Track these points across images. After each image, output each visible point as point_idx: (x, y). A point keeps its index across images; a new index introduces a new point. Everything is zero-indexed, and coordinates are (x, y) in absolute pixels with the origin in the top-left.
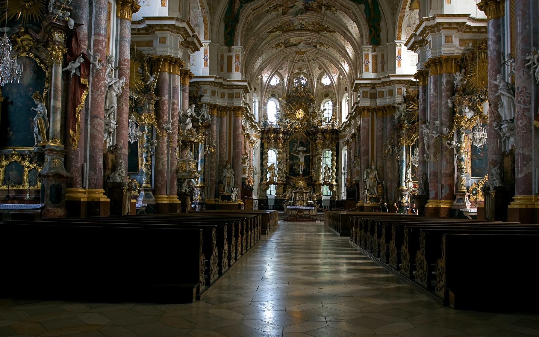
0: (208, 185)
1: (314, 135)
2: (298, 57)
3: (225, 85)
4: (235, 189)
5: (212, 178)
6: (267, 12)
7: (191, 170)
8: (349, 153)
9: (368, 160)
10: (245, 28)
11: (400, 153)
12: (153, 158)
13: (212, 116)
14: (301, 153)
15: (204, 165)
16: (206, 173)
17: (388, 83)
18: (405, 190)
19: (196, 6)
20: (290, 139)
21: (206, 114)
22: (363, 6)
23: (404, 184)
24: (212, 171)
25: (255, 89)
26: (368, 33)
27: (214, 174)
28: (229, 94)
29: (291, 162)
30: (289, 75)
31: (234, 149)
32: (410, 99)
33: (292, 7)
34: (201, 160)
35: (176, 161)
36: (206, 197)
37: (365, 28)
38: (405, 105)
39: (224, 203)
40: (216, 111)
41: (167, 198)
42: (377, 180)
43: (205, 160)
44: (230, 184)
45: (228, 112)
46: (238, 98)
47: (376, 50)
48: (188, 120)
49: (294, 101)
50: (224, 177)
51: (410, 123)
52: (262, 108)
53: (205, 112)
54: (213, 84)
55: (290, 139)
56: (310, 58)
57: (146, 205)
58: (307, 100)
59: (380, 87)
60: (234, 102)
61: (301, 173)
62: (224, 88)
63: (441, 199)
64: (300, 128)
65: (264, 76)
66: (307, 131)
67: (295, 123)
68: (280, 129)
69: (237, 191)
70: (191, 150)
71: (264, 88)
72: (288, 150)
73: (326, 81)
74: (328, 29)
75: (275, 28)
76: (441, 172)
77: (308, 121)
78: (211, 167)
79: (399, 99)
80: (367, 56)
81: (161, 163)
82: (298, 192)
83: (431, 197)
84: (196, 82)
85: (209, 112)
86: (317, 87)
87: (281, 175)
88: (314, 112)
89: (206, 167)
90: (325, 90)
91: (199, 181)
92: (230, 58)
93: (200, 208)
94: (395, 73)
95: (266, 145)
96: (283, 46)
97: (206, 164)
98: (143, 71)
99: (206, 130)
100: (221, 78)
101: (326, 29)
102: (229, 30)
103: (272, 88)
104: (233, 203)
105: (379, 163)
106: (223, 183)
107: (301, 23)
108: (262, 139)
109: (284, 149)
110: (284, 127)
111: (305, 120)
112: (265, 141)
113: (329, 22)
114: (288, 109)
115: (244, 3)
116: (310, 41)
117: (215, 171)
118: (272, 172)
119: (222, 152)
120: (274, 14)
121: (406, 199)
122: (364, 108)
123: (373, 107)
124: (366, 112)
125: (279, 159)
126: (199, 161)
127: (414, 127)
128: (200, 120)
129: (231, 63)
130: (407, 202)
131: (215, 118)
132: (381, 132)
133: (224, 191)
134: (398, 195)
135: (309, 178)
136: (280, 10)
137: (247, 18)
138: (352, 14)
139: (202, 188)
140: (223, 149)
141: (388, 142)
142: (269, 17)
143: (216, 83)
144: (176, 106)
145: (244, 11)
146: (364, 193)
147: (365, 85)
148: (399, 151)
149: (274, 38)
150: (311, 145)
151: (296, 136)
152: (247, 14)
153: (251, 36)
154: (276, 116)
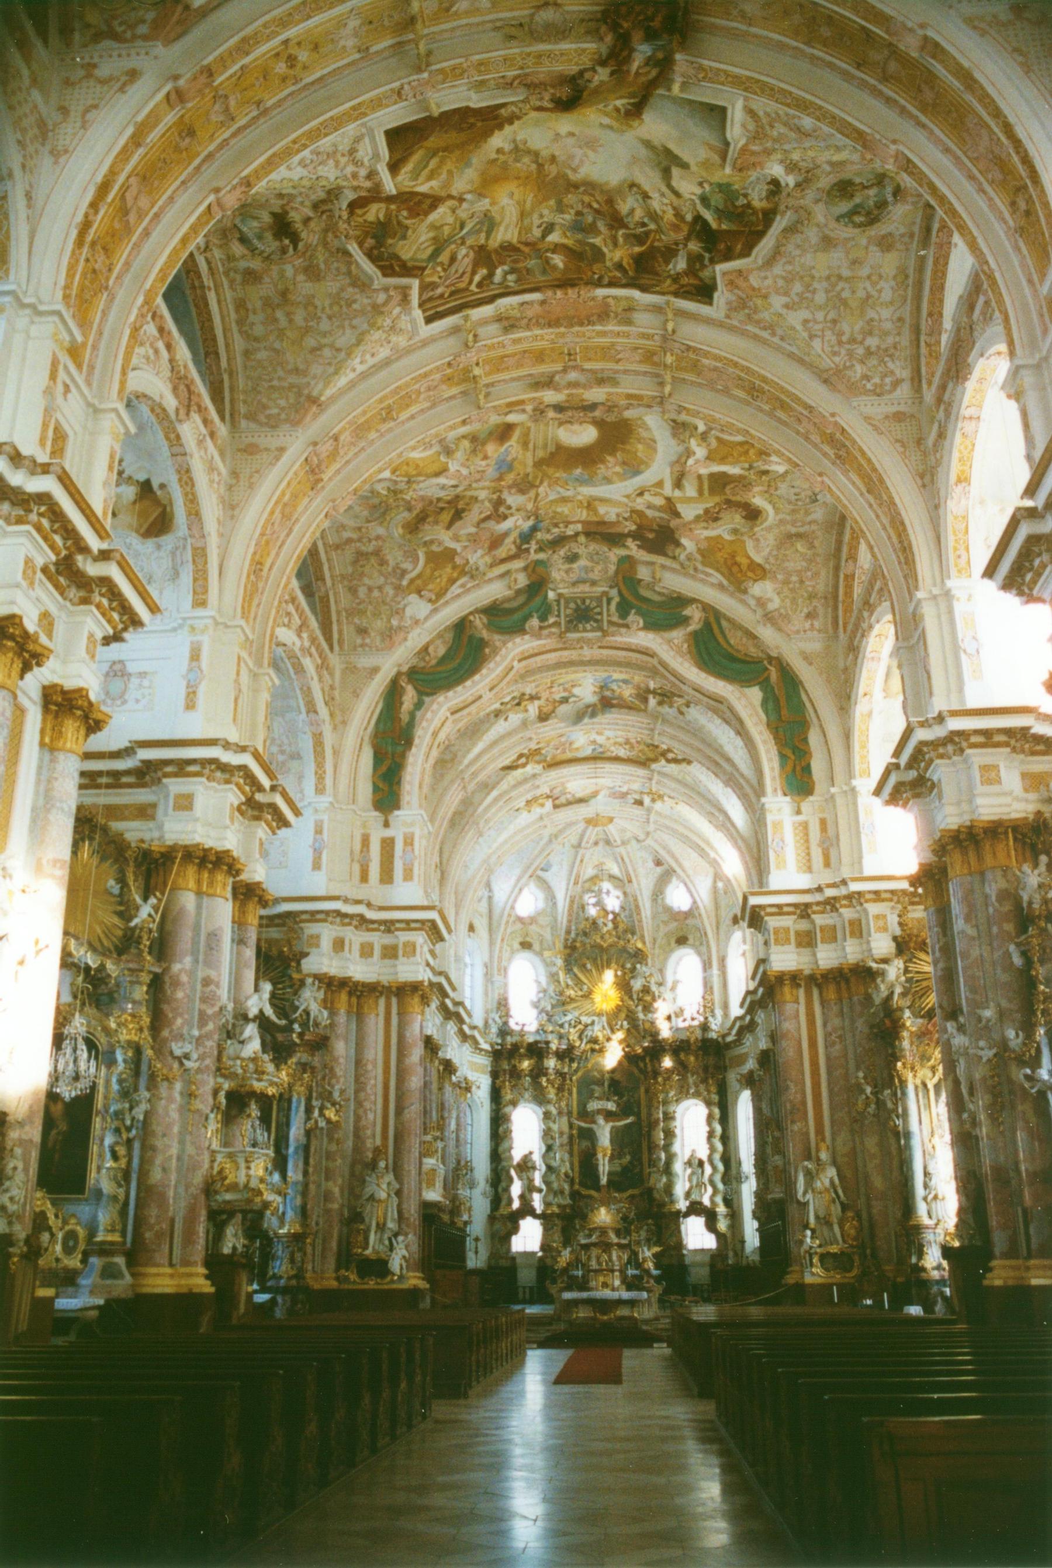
0: (315, 1229)
1: (651, 1061)
2: (592, 833)
3: (373, 922)
4: (401, 1238)
5: (330, 1206)
6: (497, 716)
7: (253, 1184)
8: (758, 1110)
9: (807, 1134)
10: (431, 761)
11: (900, 1110)
12: (137, 1145)
13: (333, 1013)
14: (601, 1120)
15: (306, 1163)
16: (312, 1187)
17: (844, 902)
18: (927, 1228)
19: (293, 703)
20: (580, 1074)
21: (314, 1008)
22: (755, 694)
23: (922, 1208)
24: (330, 1184)
25: (471, 928)
26: (776, 764)
27: (336, 1190)
28: (385, 948)
29: (585, 1144)
31: (399, 1111)
32: (912, 945)
33: (565, 700)
34: (297, 1149)
35: (206, 1158)
36: (310, 1268)
37: (768, 751)
38: (899, 964)
39: (366, 1287)
40: (344, 996)
41: (172, 1276)
42: (838, 1197)
43: (306, 1148)
44: (384, 1224)
45: (382, 1002)
46: (412, 959)
47: (803, 809)
48: (251, 1030)
50: (368, 1200)
51: (922, 1017)
52: (492, 983)
53: (310, 1000)
54: (338, 920)
55: (580, 1074)
56: (628, 835)
57: (101, 1302)
59: (822, 912)
60: (400, 968)
61: (604, 1180)
62: (368, 930)
63: (1029, 1256)
65: (495, 887)
67: (593, 1023)
68: (547, 1043)
69: (407, 1247)
70: (265, 1120)
71: (500, 924)
73: (678, 898)
74: (670, 756)
75: (521, 756)
76: (1018, 1170)
77: (631, 1017)
78: (327, 1169)
79: (882, 945)
80: (778, 825)
81: (158, 1161)
82: (594, 1245)
83: (997, 1251)
84: (289, 914)
85: (325, 1001)
86: (654, 917)
87: (555, 1186)
88: (646, 990)
89: (311, 1170)
90: (675, 924)
91: (290, 1214)
92: (388, 845)
93: (288, 1304)
94: (861, 870)
95: (508, 1095)
96: (549, 804)
97: (312, 1161)
98: (122, 888)
99: (313, 1055)
100: (358, 902)
101: (663, 754)
102: (384, 768)
103: (523, 923)
104: (394, 1286)
105: (839, 1141)
106: (363, 1221)
107: (594, 742)
108: (495, 1075)
109: (563, 1104)
110: (561, 1037)
111: (623, 1015)
112: (504, 1082)
113: (673, 738)
114: (570, 982)
115: (428, 695)
116: (624, 789)
117: (340, 1181)
119: (363, 1122)
120: (515, 718)
121: (933, 1259)
122: (781, 978)
123: (807, 972)
124: (787, 990)
125: (547, 1134)
126: (291, 1150)
127: (934, 1025)
128: (296, 1026)
129: (392, 856)
130: (939, 1267)
131: (342, 1018)
132: (838, 1047)
133: (366, 1247)
134: (910, 1243)
135: (641, 1195)
136: (533, 709)
137: (435, 734)
138: (728, 714)
139: (297, 1238)
140: (365, 1112)
141: (861, 1074)
142: (500, 727)
143: (345, 915)
144: (212, 987)
145: (429, 715)
146: (801, 1242)
147: (780, 910)
148: (896, 1104)
149: (519, 784)
150: (642, 1090)
152: (436, 723)
153: (452, 782)
154: (536, 1005)
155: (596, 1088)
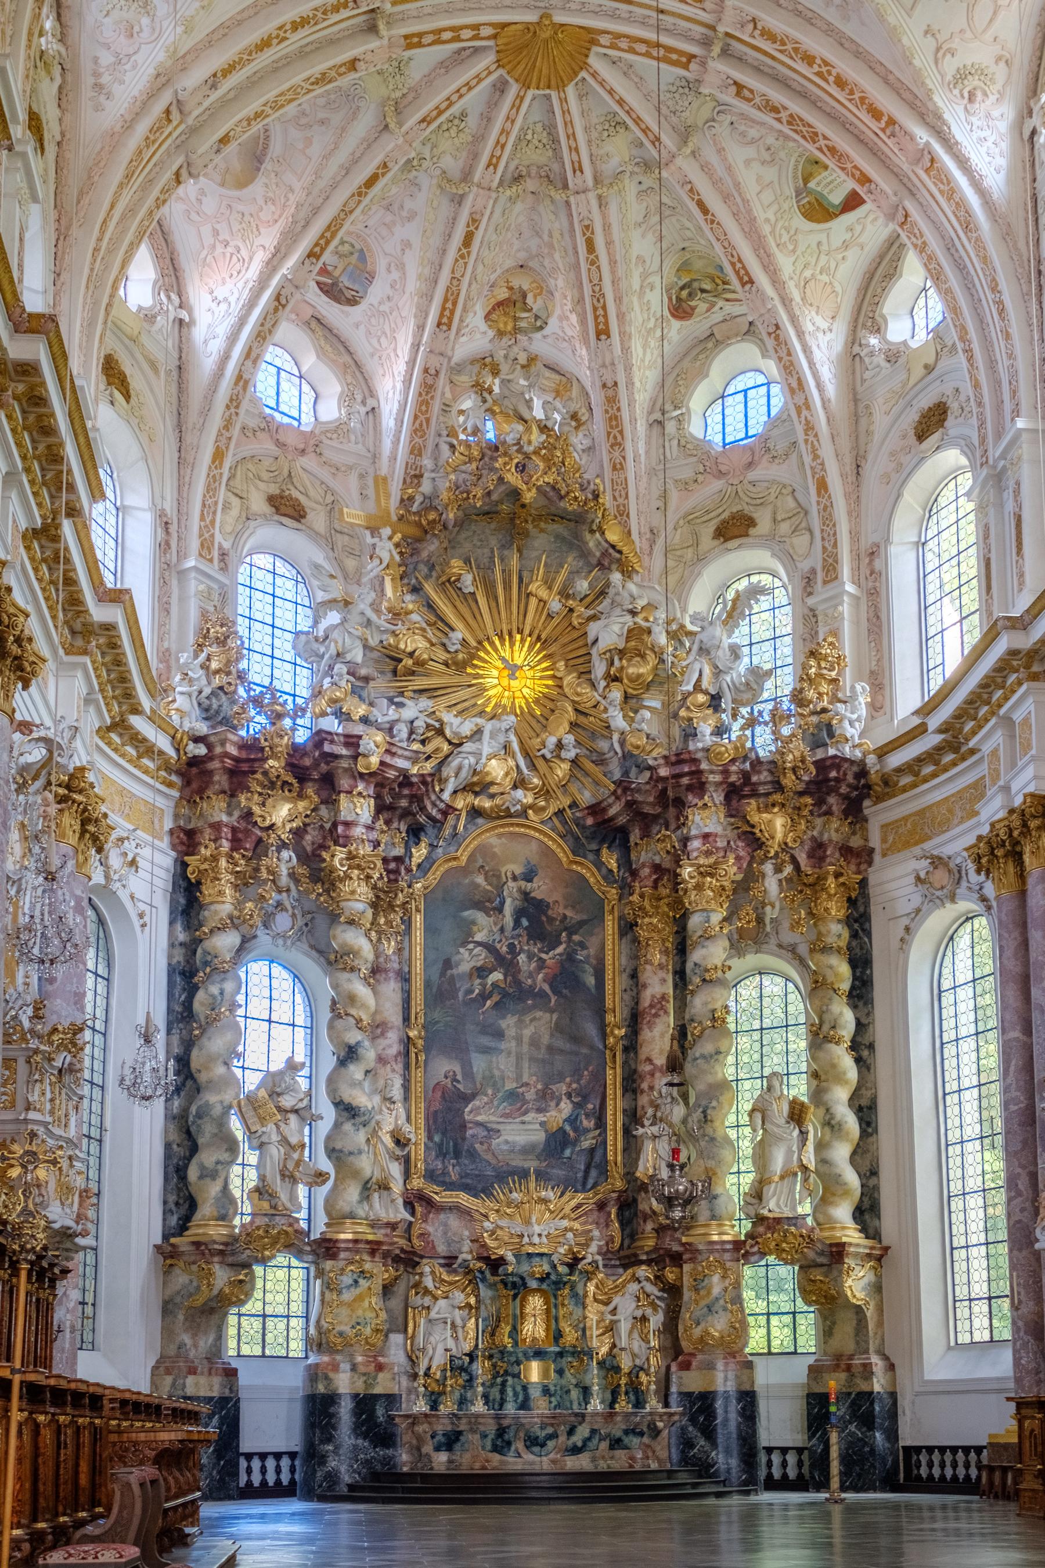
30: (421, 328)
49: (467, 561)
52: (182, 574)
55: (434, 877)
58: (571, 561)
64: (520, 783)
66: (574, 805)
67: (478, 732)
68: (352, 742)
71: (206, 411)
72: (418, 967)
87: (365, 1165)
90: (718, 485)
103: (279, 444)
109: (390, 948)
118: (284, 1141)
151: (483, 850)
155: (480, 917)
